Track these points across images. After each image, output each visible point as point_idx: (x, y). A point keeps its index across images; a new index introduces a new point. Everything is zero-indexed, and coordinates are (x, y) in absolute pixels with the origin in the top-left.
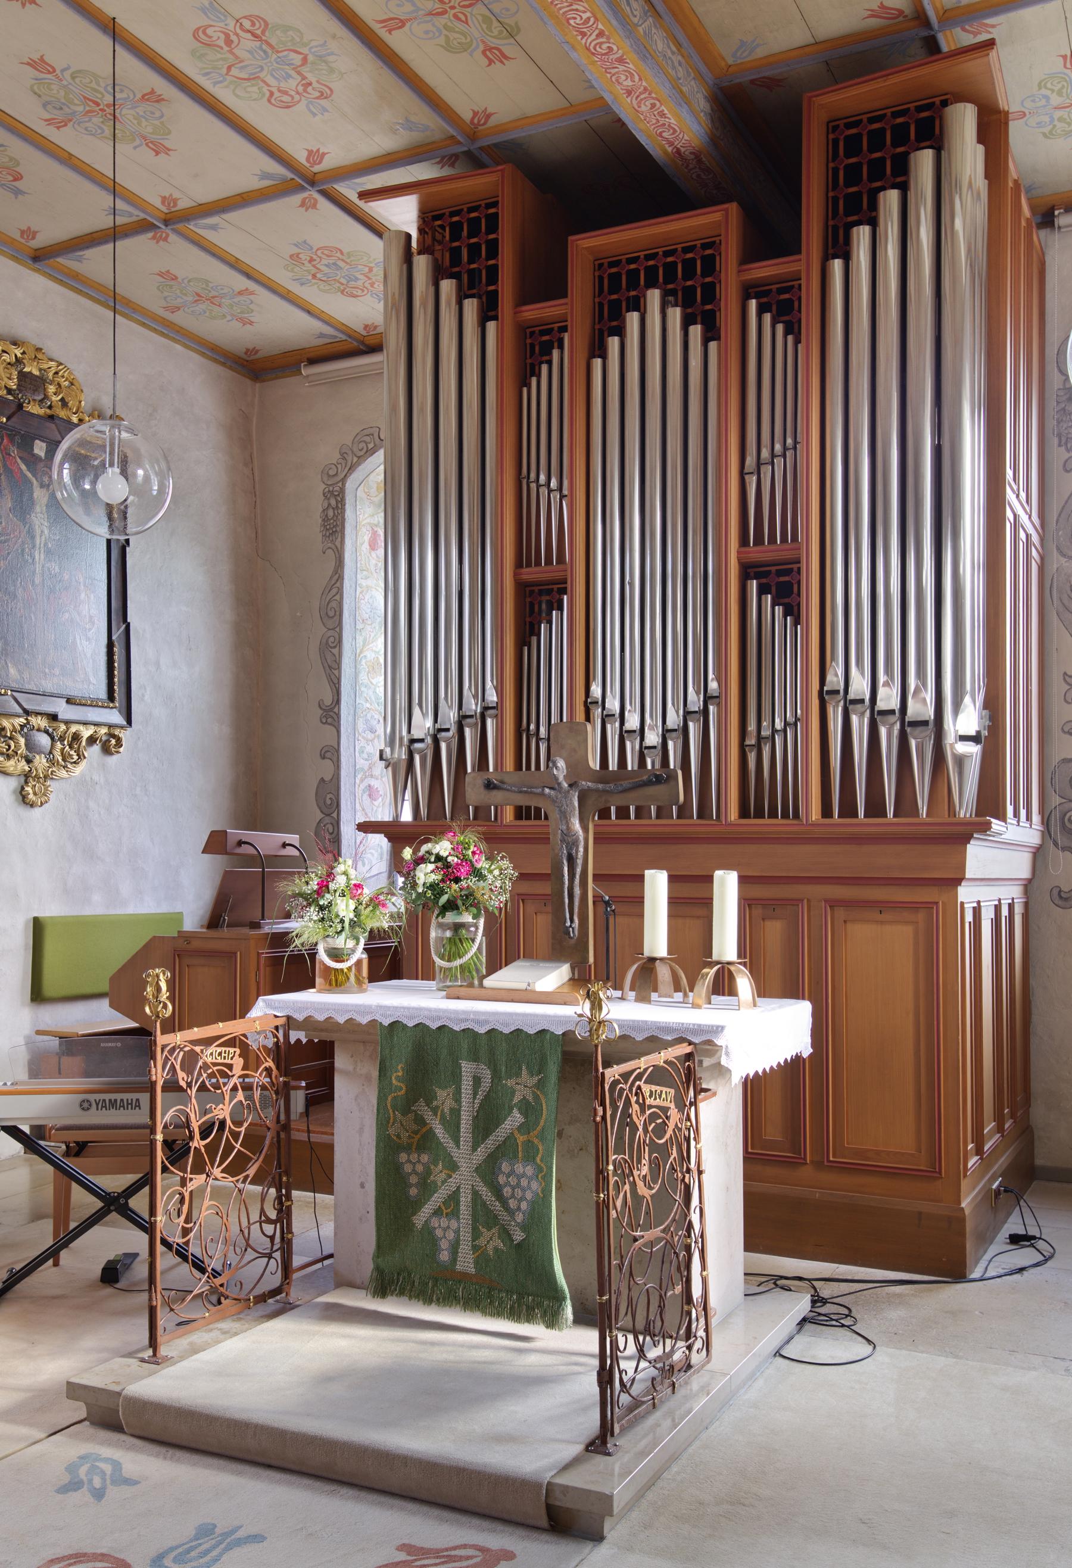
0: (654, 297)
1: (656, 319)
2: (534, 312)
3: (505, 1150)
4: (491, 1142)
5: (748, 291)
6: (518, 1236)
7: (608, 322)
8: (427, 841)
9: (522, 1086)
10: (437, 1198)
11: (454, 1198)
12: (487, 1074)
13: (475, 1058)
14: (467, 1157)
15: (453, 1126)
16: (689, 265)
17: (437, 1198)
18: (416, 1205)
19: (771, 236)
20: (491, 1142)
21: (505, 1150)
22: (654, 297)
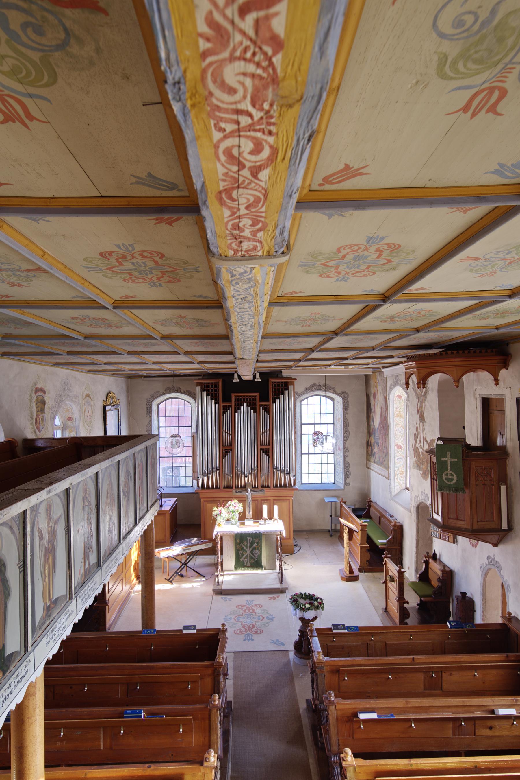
0: (245, 404)
1: (245, 408)
2: (225, 404)
3: (254, 549)
4: (252, 548)
5: (261, 406)
6: (256, 560)
7: (237, 408)
8: (228, 501)
9: (257, 540)
10: (244, 556)
11: (247, 556)
12: (251, 539)
13: (249, 537)
14: (248, 550)
15: (246, 546)
16: (250, 399)
17: (244, 556)
18: (241, 558)
19: (264, 398)
20: (252, 548)
21: (254, 549)
22: (245, 404)
